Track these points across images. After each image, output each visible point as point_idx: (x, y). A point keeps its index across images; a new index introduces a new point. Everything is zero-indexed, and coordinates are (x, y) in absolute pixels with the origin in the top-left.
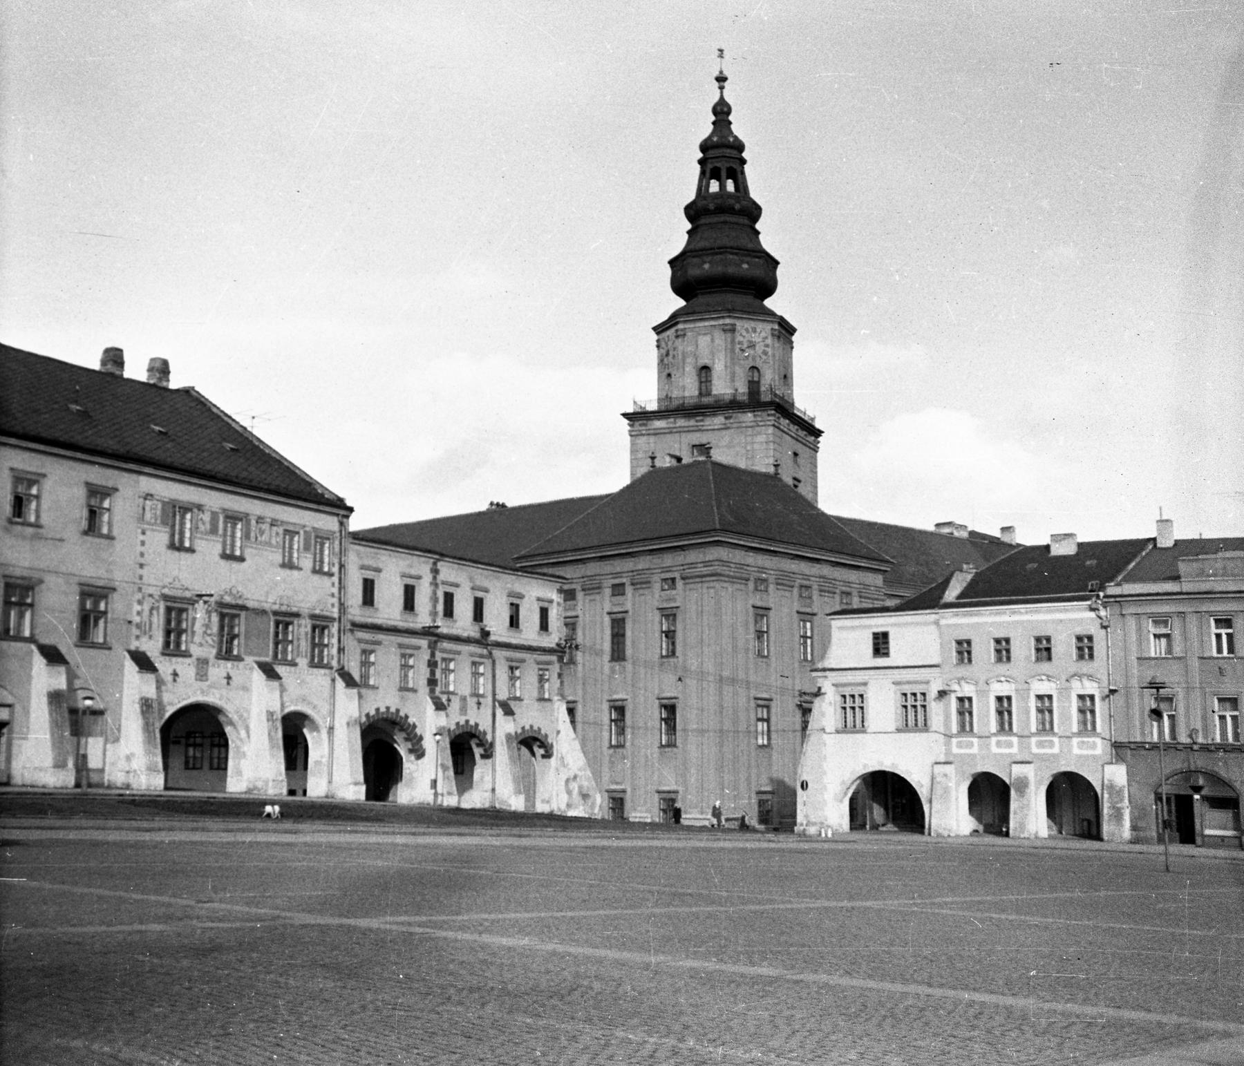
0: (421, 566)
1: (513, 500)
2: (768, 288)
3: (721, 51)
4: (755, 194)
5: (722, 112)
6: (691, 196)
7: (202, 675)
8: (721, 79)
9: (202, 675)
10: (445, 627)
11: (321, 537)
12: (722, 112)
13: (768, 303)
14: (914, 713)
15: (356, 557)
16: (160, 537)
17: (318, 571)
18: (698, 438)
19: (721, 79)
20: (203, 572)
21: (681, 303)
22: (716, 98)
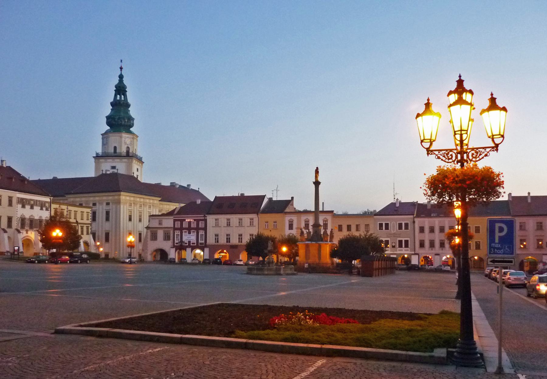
1: (59, 177)
2: (132, 126)
3: (121, 61)
4: (130, 100)
5: (121, 77)
6: (112, 100)
7: (27, 233)
8: (121, 68)
9: (27, 233)
12: (121, 77)
13: (131, 129)
14: (167, 237)
16: (20, 206)
18: (114, 165)
19: (121, 68)
20: (27, 212)
21: (109, 128)
22: (119, 73)
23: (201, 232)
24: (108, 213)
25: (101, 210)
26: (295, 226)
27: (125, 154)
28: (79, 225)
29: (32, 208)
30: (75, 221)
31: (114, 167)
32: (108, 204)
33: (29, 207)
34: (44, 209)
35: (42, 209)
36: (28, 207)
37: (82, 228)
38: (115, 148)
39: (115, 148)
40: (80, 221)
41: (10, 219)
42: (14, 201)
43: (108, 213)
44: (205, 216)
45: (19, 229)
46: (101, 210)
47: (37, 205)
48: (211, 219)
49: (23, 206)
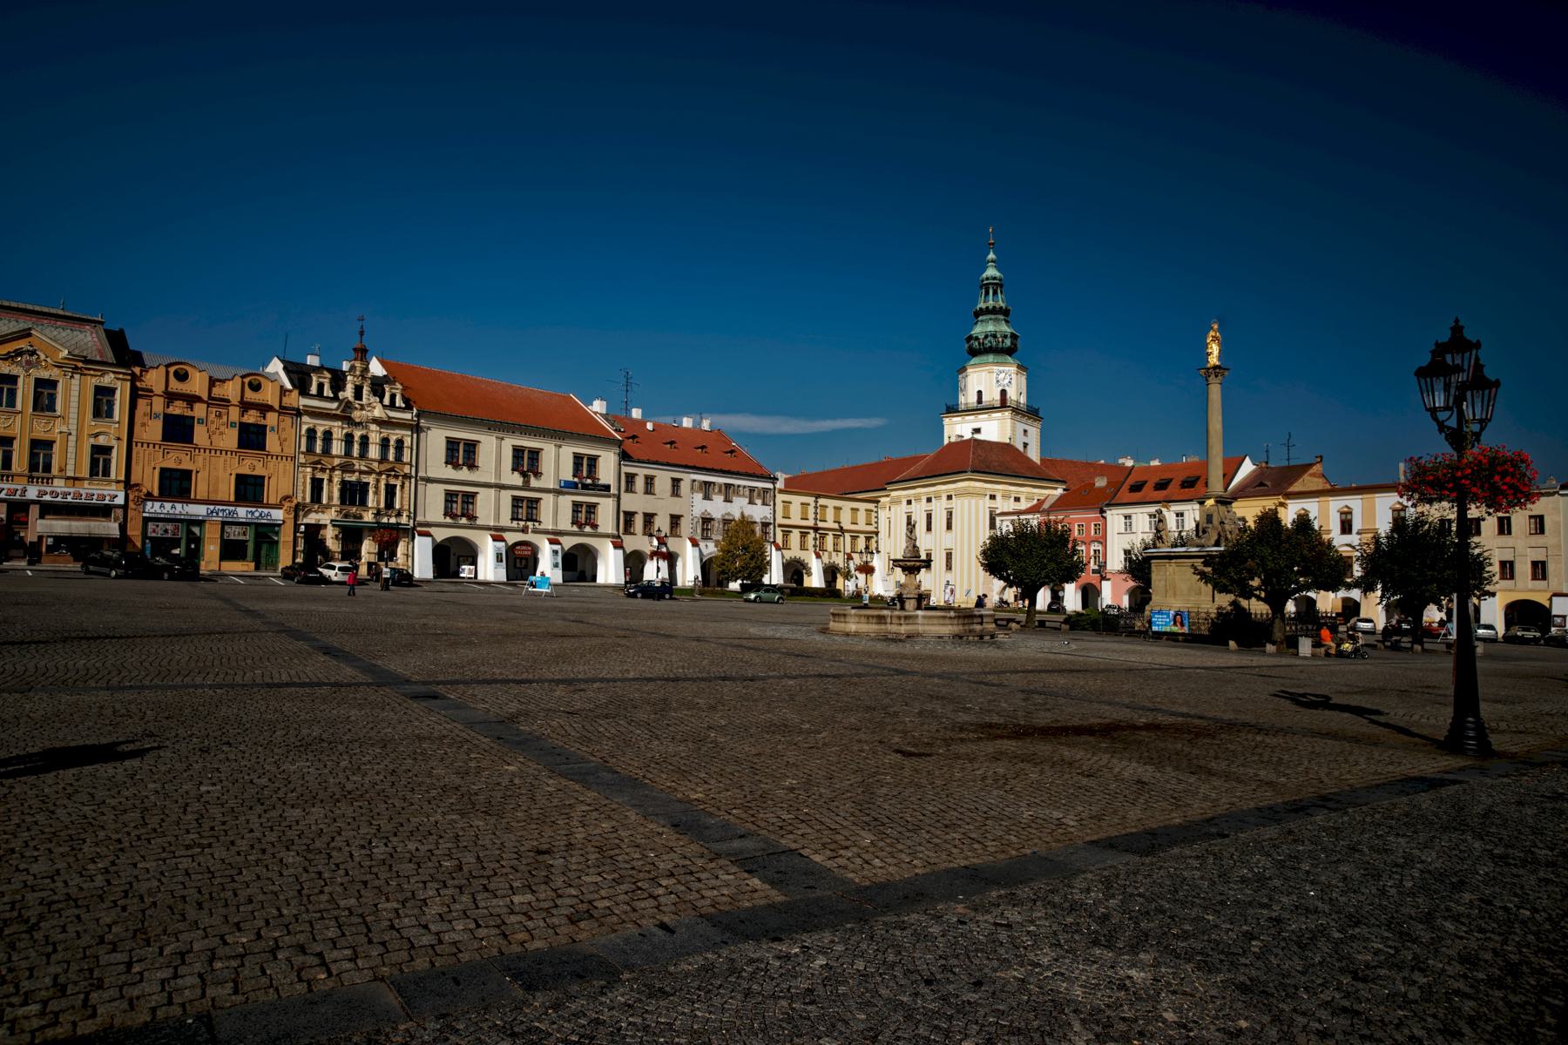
0: (811, 500)
10: (820, 524)
11: (766, 490)
15: (780, 498)
16: (699, 496)
17: (764, 504)
18: (976, 425)
23: (1095, 546)
24: (950, 514)
25: (939, 509)
26: (1355, 528)
27: (998, 404)
28: (847, 535)
29: (728, 500)
30: (836, 526)
31: (977, 431)
32: (949, 497)
33: (722, 498)
34: (759, 502)
35: (751, 502)
36: (718, 499)
37: (854, 538)
38: (980, 393)
39: (980, 393)
40: (847, 525)
41: (675, 520)
42: (685, 487)
43: (950, 514)
44: (1102, 512)
45: (698, 537)
46: (939, 509)
47: (738, 495)
48: (1115, 518)
49: (707, 497)
